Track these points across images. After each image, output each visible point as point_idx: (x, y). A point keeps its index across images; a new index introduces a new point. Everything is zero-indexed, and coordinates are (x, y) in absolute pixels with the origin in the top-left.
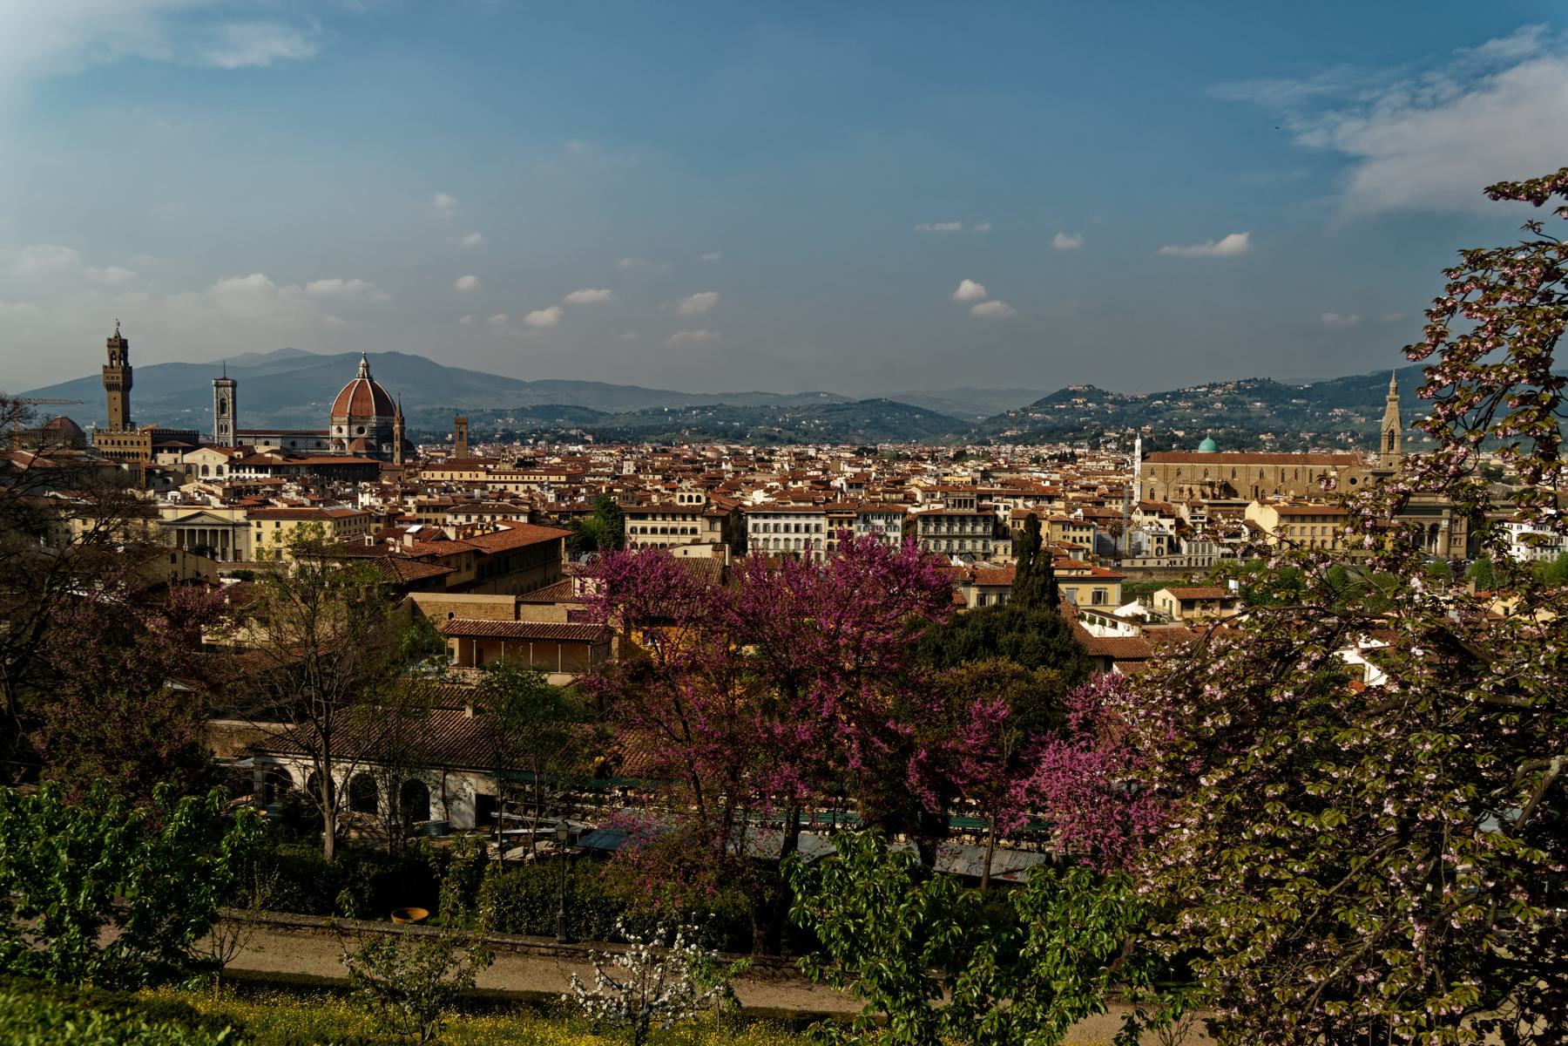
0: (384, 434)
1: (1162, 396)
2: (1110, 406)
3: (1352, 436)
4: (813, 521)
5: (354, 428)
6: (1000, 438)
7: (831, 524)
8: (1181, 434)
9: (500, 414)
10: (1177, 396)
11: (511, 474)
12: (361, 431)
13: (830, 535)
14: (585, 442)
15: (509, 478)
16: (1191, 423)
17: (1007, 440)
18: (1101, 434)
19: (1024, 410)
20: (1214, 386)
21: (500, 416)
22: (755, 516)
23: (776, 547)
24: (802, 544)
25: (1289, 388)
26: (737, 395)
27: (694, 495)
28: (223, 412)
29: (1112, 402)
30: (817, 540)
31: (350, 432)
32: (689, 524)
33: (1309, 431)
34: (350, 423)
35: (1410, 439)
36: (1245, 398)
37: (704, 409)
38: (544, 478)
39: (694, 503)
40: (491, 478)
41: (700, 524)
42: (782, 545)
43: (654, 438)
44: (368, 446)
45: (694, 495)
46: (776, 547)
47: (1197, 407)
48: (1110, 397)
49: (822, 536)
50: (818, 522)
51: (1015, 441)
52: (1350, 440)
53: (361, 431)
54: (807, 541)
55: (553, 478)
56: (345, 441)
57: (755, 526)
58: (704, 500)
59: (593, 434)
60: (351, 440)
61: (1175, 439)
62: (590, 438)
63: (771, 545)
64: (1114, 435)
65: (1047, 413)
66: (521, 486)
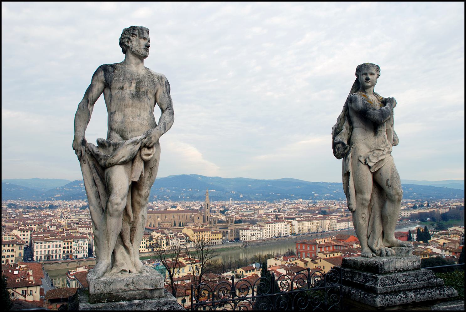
4: (58, 243)
6: (54, 197)
7: (65, 244)
13: (64, 248)
17: (58, 199)
19: (62, 187)
24: (54, 252)
30: (60, 250)
35: (184, 197)
42: (47, 253)
49: (62, 248)
50: (60, 244)
51: (62, 199)
52: (168, 198)
54: (56, 250)
63: (43, 253)
65: (70, 188)
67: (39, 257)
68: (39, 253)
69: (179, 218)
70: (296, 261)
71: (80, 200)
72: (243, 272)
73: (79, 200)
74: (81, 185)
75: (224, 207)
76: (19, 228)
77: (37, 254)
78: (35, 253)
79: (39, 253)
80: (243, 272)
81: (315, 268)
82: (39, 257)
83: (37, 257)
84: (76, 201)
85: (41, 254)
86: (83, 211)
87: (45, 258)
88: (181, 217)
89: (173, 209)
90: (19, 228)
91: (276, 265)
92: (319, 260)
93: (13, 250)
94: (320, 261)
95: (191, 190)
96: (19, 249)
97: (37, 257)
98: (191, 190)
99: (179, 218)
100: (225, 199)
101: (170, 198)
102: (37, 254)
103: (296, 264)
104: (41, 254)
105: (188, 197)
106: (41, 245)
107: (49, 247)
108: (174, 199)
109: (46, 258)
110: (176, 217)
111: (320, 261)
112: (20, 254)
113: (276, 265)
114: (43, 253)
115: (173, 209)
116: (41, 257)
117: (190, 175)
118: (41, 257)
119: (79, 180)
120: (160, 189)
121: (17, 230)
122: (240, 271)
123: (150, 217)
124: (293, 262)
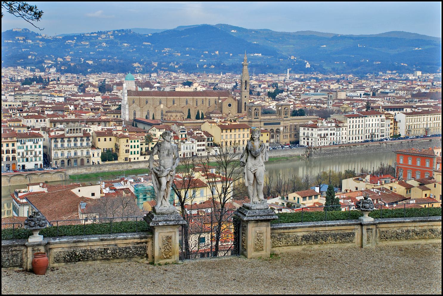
1: (71, 37)
2: (41, 43)
3: (177, 64)
8: (90, 62)
10: (81, 37)
16: (90, 54)
18: (42, 62)
20: (100, 33)
25: (141, 36)
29: (41, 40)
33: (155, 62)
35: (205, 66)
36: (117, 41)
47: (92, 45)
48: (40, 37)
52: (176, 67)
61: (89, 66)
64: (50, 62)
69: (197, 105)
70: (391, 185)
71: (20, 67)
72: (298, 198)
73: (18, 67)
74: (19, 40)
75: (275, 85)
80: (298, 198)
81: (424, 197)
84: (12, 69)
86: (28, 88)
88: (200, 103)
89: (187, 89)
91: (357, 189)
92: (433, 184)
94: (435, 187)
95: (217, 52)
98: (217, 52)
99: (197, 105)
100: (278, 70)
101: (180, 67)
103: (391, 189)
105: (213, 67)
108: (188, 69)
110: (191, 103)
111: (435, 187)
113: (357, 189)
115: (187, 89)
117: (217, 25)
119: (14, 30)
120: (163, 51)
122: (294, 198)
123: (147, 102)
124: (387, 186)
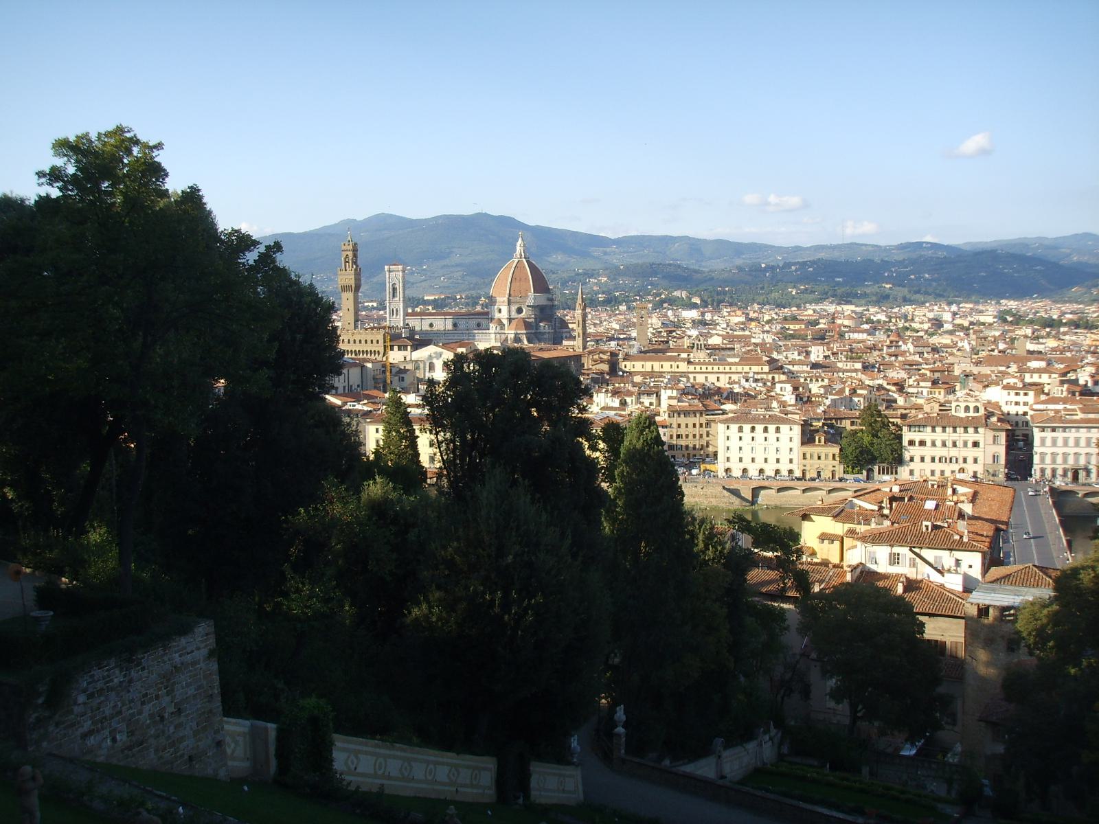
0: (545, 312)
5: (514, 308)
9: (590, 274)
11: (704, 363)
12: (519, 311)
14: (694, 306)
15: (710, 368)
21: (591, 276)
22: (1043, 429)
23: (1065, 461)
26: (833, 248)
27: (972, 406)
28: (394, 296)
31: (509, 311)
32: (971, 436)
34: (509, 303)
37: (803, 264)
38: (746, 369)
39: (971, 414)
40: (691, 368)
41: (983, 435)
42: (1071, 461)
43: (760, 299)
44: (527, 325)
45: (972, 406)
46: (1065, 461)
53: (519, 311)
55: (756, 369)
56: (505, 322)
57: (1043, 440)
58: (982, 412)
59: (700, 296)
60: (510, 320)
62: (696, 300)
63: (1059, 459)
66: (722, 376)
67: (1048, 473)
68: (1048, 459)
76: (1005, 382)
77: (1042, 460)
78: (1036, 459)
79: (1048, 459)
82: (1048, 473)
83: (1043, 471)
85: (1054, 461)
87: (1065, 475)
90: (1005, 382)
93: (976, 444)
96: (992, 443)
97: (1043, 471)
102: (1042, 460)
104: (1054, 461)
106: (1054, 434)
107: (1077, 441)
109: (1070, 474)
112: (995, 458)
114: (1059, 459)
116: (1054, 471)
118: (1054, 471)
121: (1000, 387)
